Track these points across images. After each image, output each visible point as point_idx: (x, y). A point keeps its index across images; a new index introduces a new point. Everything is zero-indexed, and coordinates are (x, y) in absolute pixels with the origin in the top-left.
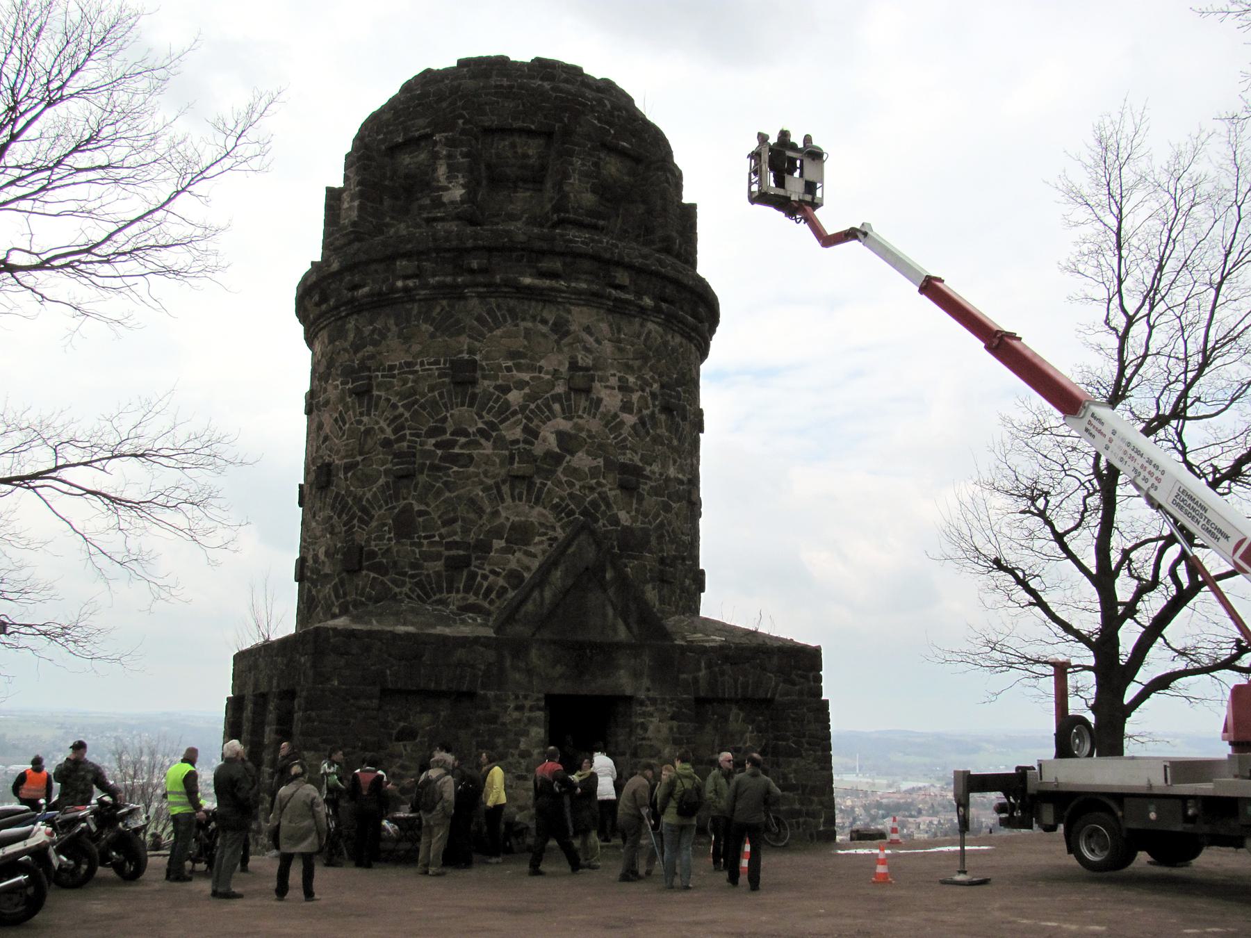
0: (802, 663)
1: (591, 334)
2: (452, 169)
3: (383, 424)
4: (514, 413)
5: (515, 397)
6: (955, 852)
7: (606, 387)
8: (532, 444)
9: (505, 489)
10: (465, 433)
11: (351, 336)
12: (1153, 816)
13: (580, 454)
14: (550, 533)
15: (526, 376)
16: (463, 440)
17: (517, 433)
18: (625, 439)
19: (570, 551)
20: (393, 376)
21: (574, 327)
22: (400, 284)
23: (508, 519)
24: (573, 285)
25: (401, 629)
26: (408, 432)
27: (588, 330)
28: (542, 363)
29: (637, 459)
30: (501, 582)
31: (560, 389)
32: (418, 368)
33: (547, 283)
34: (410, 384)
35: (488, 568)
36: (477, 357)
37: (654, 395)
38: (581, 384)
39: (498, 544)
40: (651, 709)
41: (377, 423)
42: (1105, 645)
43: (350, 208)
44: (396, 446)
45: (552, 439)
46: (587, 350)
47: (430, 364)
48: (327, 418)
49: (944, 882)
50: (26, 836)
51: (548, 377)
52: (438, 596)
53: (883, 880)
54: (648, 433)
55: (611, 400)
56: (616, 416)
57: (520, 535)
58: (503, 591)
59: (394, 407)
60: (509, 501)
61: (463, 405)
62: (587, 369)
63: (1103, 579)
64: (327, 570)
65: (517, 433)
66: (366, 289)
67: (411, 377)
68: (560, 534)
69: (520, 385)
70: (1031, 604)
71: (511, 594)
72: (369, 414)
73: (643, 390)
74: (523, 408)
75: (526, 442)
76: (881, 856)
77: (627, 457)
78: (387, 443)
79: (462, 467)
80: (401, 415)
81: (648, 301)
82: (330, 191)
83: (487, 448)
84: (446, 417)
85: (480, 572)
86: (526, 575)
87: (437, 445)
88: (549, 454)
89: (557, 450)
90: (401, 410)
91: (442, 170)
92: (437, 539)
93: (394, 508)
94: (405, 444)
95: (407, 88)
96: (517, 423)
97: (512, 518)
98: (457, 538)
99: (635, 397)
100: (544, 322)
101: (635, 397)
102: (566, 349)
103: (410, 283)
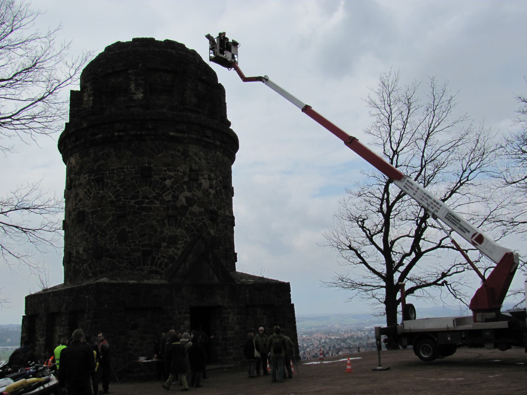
0: (283, 289)
1: (197, 157)
2: (137, 86)
3: (110, 194)
4: (168, 189)
5: (168, 182)
7: (204, 178)
8: (176, 202)
9: (166, 221)
10: (148, 198)
11: (92, 156)
12: (449, 339)
13: (195, 206)
14: (185, 239)
15: (172, 174)
16: (147, 201)
17: (170, 198)
18: (211, 200)
19: (195, 246)
20: (114, 173)
21: (190, 154)
22: (116, 134)
23: (167, 234)
24: (190, 136)
25: (131, 282)
26: (122, 197)
27: (196, 154)
28: (179, 168)
29: (216, 208)
30: (166, 260)
31: (186, 179)
32: (125, 170)
33: (180, 135)
34: (122, 177)
35: (159, 254)
36: (152, 166)
37: (220, 181)
38: (194, 177)
39: (164, 244)
40: (230, 311)
41: (108, 193)
42: (388, 278)
43: (88, 100)
44: (117, 203)
45: (184, 200)
46: (197, 163)
47: (131, 168)
48: (81, 192)
49: (373, 370)
50: (48, 381)
51: (181, 174)
52: (139, 267)
53: (350, 371)
54: (219, 198)
55: (205, 184)
56: (207, 190)
57: (173, 241)
58: (167, 264)
59: (115, 187)
60: (167, 226)
61: (146, 186)
62: (196, 171)
63: (387, 251)
64: (85, 257)
65: (170, 198)
66: (100, 136)
67: (122, 174)
68: (189, 239)
69: (170, 177)
70: (361, 263)
71: (170, 265)
72: (103, 190)
73: (217, 180)
74: (172, 187)
75: (173, 201)
76: (349, 362)
77: (214, 207)
78: (112, 202)
79: (146, 212)
80: (119, 190)
81: (218, 143)
82: (72, 92)
83: (158, 204)
84: (139, 191)
85: (157, 256)
86: (176, 257)
87: (136, 203)
88: (183, 206)
89: (186, 205)
90: (118, 188)
91: (133, 86)
92: (137, 243)
93: (117, 230)
94: (121, 203)
95: (108, 49)
96: (170, 193)
97: (169, 233)
98: (146, 242)
99: (214, 182)
100: (179, 151)
101: (214, 182)
102: (188, 163)
103: (121, 134)
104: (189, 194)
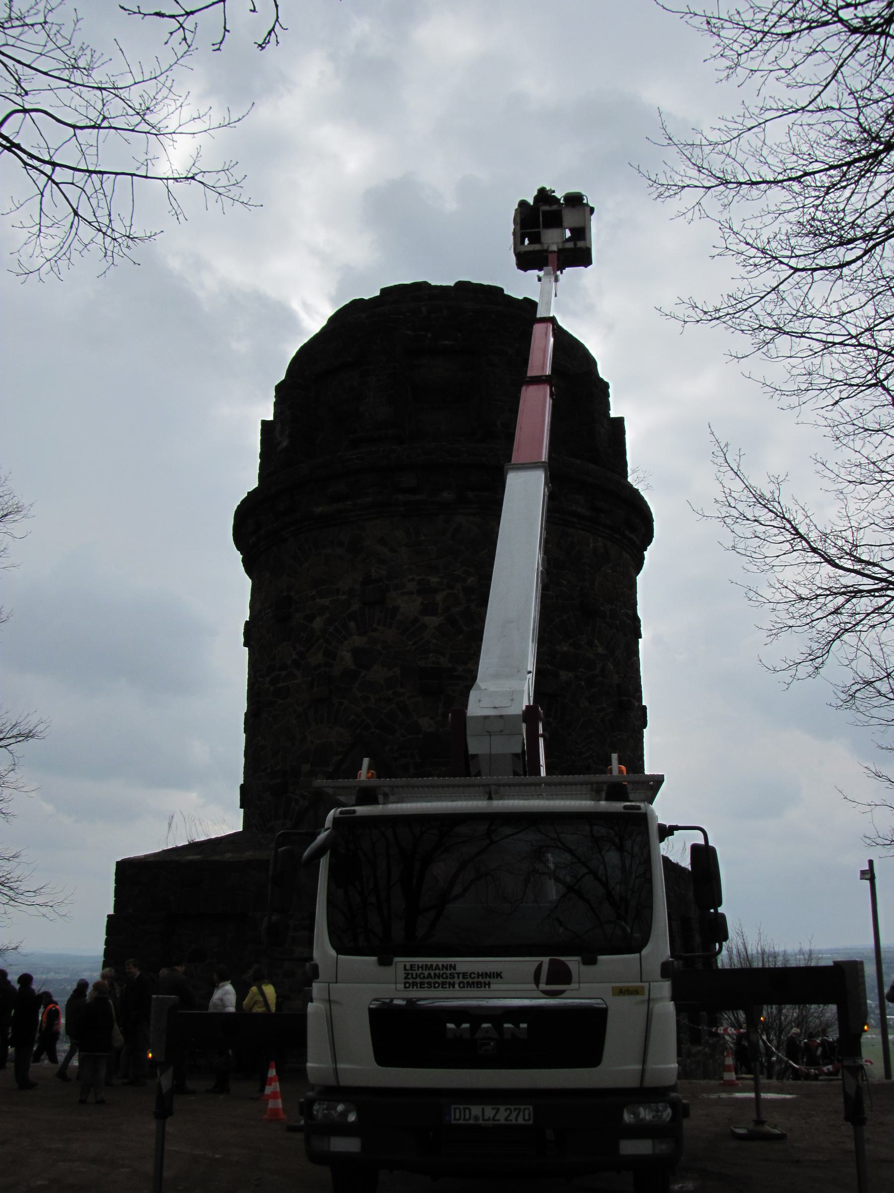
5: (318, 623)
6: (749, 1099)
16: (284, 673)
39: (306, 768)
45: (348, 656)
51: (344, 597)
89: (353, 667)
101: (439, 597)
104: (358, 641)
